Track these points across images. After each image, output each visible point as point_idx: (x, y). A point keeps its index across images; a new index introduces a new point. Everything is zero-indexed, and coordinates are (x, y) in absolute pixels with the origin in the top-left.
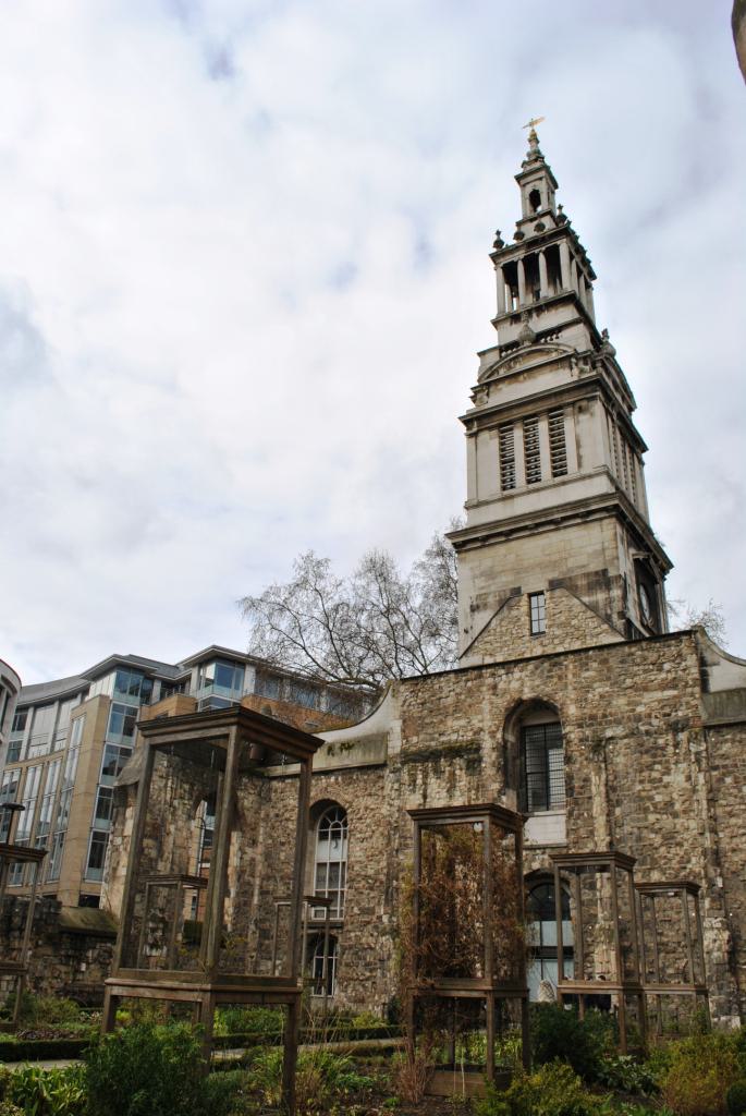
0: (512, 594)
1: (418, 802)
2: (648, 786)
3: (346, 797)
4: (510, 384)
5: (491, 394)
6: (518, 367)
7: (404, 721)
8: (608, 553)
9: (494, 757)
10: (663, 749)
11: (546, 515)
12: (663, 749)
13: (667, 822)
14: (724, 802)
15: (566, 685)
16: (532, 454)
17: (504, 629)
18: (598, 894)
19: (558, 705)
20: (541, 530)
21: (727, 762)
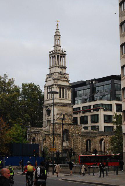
6: (62, 79)
16: (63, 94)
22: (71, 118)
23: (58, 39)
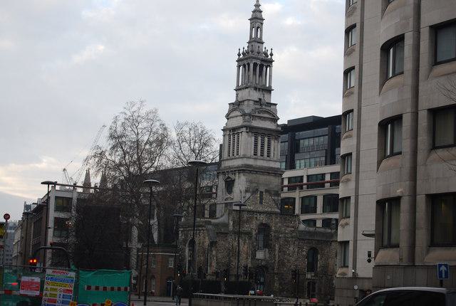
6: (261, 115)
23: (258, 28)
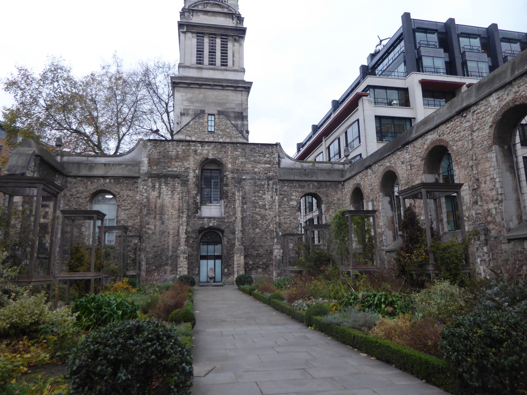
0: (201, 112)
1: (157, 195)
2: (257, 198)
3: (116, 190)
4: (204, 14)
5: (194, 16)
6: (208, 9)
7: (149, 159)
8: (243, 105)
9: (194, 180)
10: (263, 185)
11: (219, 82)
12: (263, 185)
13: (263, 211)
14: (283, 207)
15: (227, 157)
16: (212, 52)
17: (196, 126)
18: (237, 236)
19: (224, 163)
20: (215, 88)
21: (285, 193)
22: (243, 125)
